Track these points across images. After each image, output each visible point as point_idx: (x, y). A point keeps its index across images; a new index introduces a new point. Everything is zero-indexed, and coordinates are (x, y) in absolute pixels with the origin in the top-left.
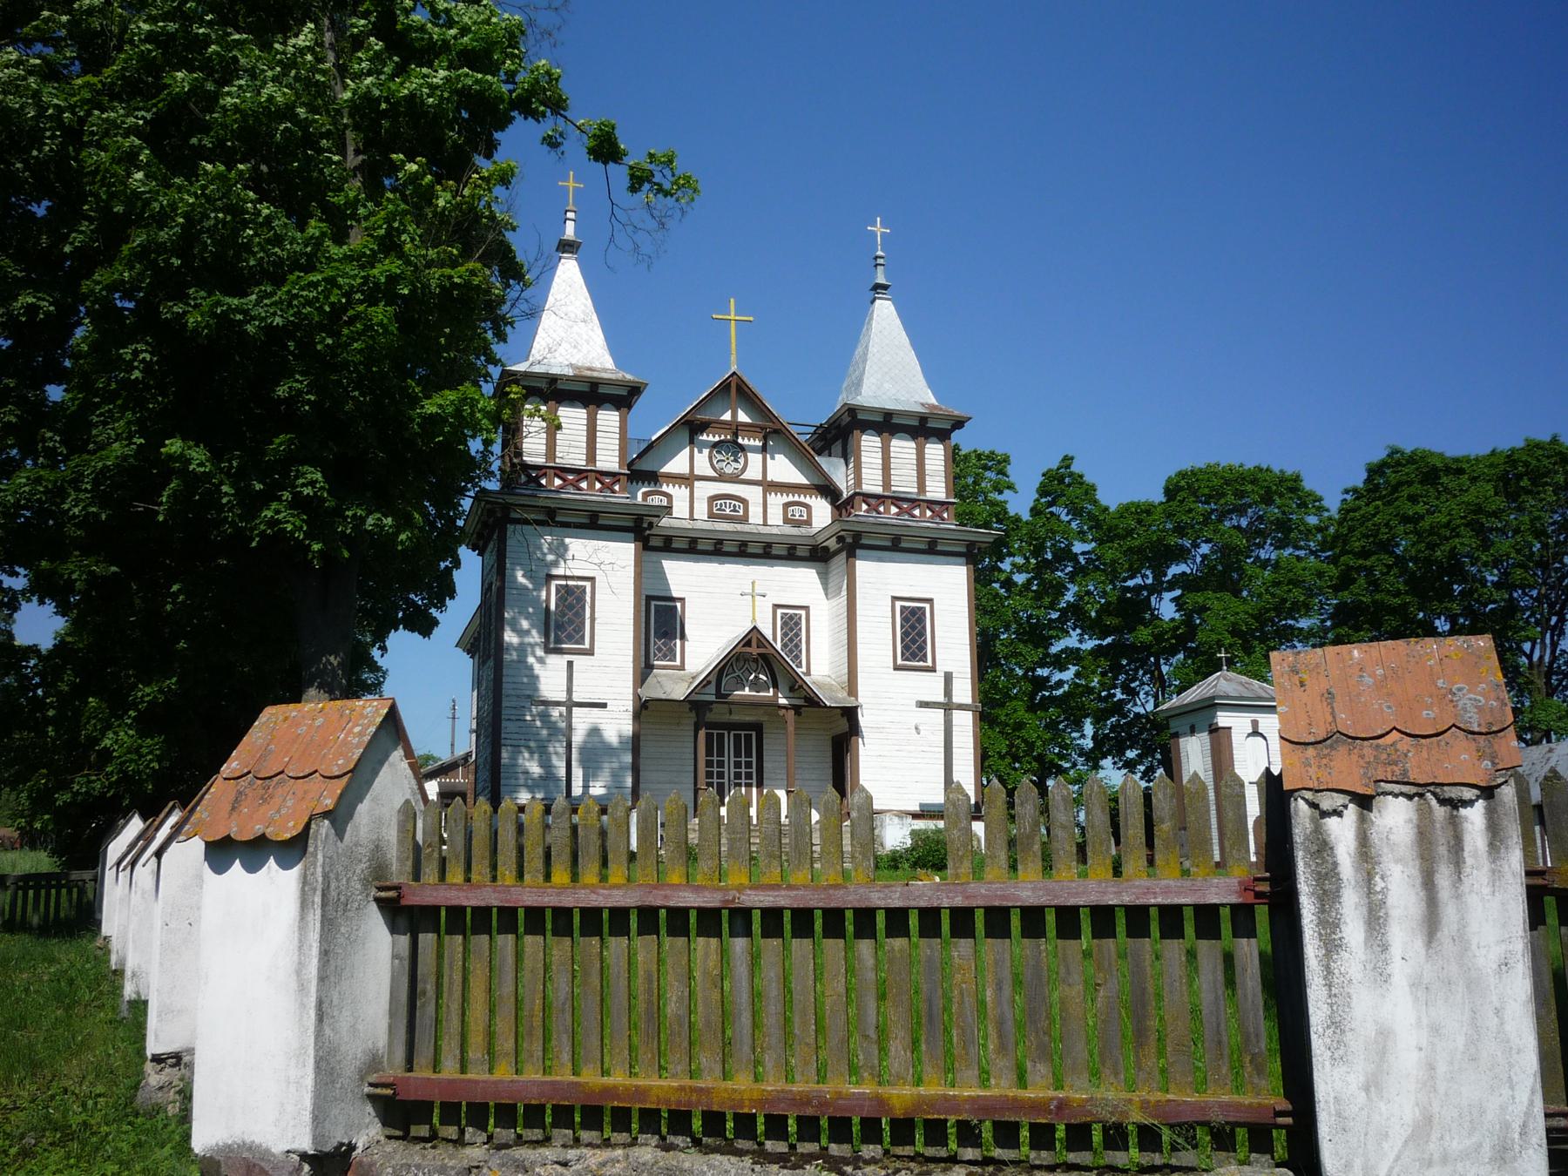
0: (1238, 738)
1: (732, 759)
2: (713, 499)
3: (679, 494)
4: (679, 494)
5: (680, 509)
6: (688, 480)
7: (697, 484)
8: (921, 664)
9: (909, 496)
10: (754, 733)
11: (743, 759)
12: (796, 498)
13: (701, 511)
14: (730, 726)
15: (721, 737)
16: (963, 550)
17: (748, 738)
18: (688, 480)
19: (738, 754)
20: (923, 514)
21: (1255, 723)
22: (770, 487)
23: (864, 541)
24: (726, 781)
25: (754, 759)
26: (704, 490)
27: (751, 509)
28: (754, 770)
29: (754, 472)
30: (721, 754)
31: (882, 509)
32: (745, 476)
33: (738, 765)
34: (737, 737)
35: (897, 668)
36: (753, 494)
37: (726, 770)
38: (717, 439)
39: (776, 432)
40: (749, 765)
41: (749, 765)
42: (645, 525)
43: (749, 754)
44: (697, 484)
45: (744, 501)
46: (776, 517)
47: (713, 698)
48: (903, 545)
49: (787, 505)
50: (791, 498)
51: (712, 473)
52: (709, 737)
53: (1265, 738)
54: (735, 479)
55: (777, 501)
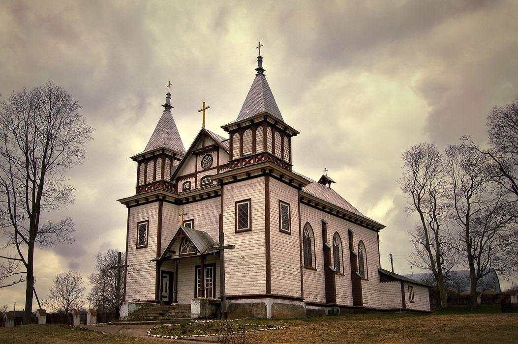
2: (202, 179)
3: (192, 180)
5: (193, 188)
8: (246, 228)
9: (248, 156)
10: (213, 267)
13: (199, 183)
17: (211, 269)
18: (194, 175)
20: (255, 161)
25: (213, 278)
26: (200, 176)
31: (239, 165)
35: (237, 232)
40: (211, 280)
41: (211, 280)
43: (211, 276)
47: (178, 257)
48: (252, 175)
51: (202, 169)
54: (209, 169)
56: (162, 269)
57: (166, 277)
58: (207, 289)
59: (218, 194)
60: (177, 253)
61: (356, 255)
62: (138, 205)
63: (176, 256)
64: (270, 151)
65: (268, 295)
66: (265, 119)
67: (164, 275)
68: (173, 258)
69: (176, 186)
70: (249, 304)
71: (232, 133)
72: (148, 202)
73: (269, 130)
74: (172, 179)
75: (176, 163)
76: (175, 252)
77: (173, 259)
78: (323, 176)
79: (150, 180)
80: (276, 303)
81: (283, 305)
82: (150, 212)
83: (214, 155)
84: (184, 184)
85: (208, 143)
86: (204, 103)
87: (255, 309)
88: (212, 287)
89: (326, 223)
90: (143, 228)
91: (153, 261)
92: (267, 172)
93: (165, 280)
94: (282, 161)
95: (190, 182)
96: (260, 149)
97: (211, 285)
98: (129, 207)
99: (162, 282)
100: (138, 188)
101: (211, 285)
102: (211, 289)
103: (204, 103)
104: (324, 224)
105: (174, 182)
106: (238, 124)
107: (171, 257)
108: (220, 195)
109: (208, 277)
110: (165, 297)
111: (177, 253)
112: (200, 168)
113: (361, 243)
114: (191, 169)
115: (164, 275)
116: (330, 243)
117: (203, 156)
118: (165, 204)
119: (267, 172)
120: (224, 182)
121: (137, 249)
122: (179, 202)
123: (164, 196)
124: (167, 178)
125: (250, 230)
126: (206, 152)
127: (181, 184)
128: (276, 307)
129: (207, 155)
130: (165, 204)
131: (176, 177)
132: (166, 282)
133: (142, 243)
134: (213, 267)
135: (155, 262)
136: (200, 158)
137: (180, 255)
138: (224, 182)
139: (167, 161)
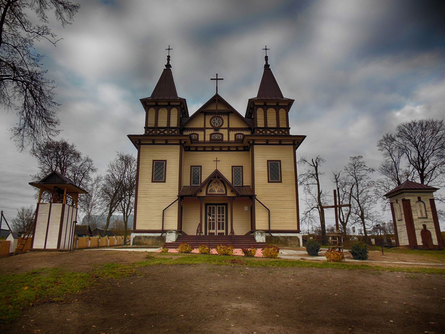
0: (412, 203)
1: (217, 215)
3: (201, 134)
4: (201, 134)
5: (201, 138)
6: (203, 129)
7: (206, 130)
10: (225, 206)
11: (221, 215)
12: (239, 132)
14: (216, 204)
15: (214, 208)
16: (292, 143)
17: (223, 208)
18: (203, 129)
19: (219, 213)
22: (230, 129)
23: (256, 142)
24: (215, 222)
27: (224, 136)
28: (225, 218)
29: (225, 125)
30: (214, 213)
32: (223, 127)
33: (219, 216)
34: (219, 208)
36: (224, 132)
37: (215, 218)
38: (213, 116)
39: (232, 112)
40: (223, 216)
41: (223, 216)
42: (183, 142)
43: (223, 213)
44: (206, 130)
45: (222, 135)
46: (232, 138)
47: (205, 195)
49: (236, 135)
50: (237, 132)
51: (210, 126)
52: (210, 208)
53: (424, 203)
55: (232, 134)
58: (219, 223)
63: (203, 194)
68: (198, 195)
70: (284, 236)
76: (201, 191)
77: (198, 197)
83: (225, 118)
85: (221, 108)
86: (217, 74)
88: (225, 222)
95: (198, 135)
97: (223, 220)
100: (146, 128)
101: (223, 220)
102: (223, 223)
103: (217, 74)
112: (208, 125)
117: (211, 116)
120: (255, 143)
121: (152, 182)
125: (281, 182)
126: (217, 114)
134: (225, 206)
136: (208, 118)
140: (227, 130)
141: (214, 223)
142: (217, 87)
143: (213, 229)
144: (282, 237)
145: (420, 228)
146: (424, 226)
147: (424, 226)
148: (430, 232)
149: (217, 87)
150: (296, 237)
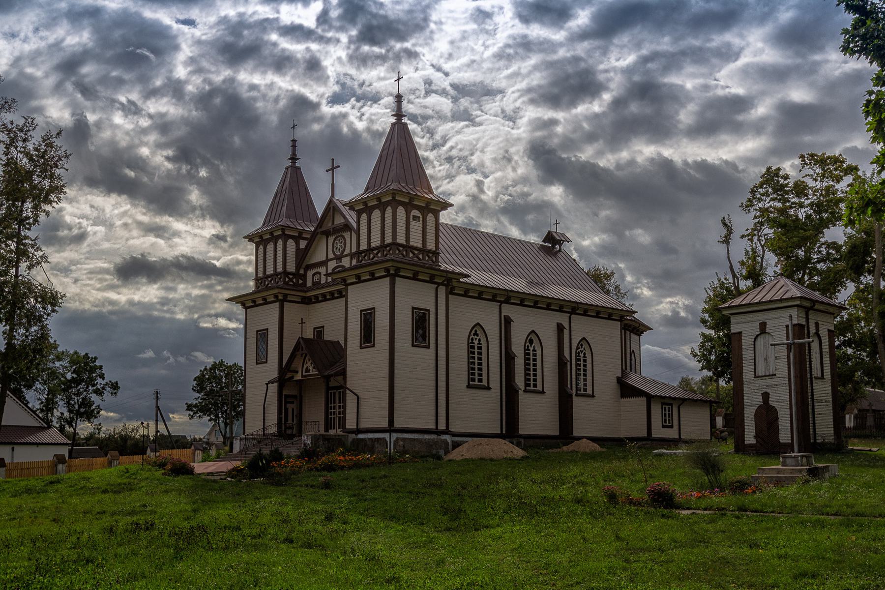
15: (334, 393)
21: (763, 326)
29: (347, 252)
47: (300, 378)
51: (333, 256)
56: (285, 393)
57: (293, 403)
58: (340, 417)
59: (342, 294)
60: (300, 374)
61: (566, 363)
62: (256, 306)
63: (298, 377)
64: (401, 240)
65: (391, 428)
66: (394, 198)
67: (288, 400)
69: (304, 277)
71: (359, 213)
72: (266, 302)
73: (401, 211)
74: (298, 267)
75: (303, 244)
76: (297, 372)
77: (297, 381)
78: (549, 232)
79: (270, 271)
80: (400, 438)
81: (414, 439)
82: (269, 316)
84: (314, 275)
87: (376, 446)
89: (510, 323)
90: (263, 335)
91: (270, 382)
92: (391, 272)
93: (290, 406)
94: (424, 251)
95: (319, 273)
96: (388, 240)
98: (246, 308)
99: (286, 410)
104: (508, 321)
105: (302, 272)
106: (364, 202)
107: (293, 377)
108: (343, 296)
109: (340, 403)
110: (292, 428)
111: (300, 374)
112: (331, 256)
113: (585, 345)
114: (319, 255)
115: (288, 400)
116: (518, 348)
118: (286, 304)
119: (391, 272)
122: (307, 301)
123: (285, 296)
124: (291, 267)
127: (310, 274)
128: (401, 443)
129: (339, 236)
130: (286, 304)
131: (304, 265)
132: (293, 409)
133: (261, 359)
135: (276, 384)
136: (331, 239)
137: (303, 376)
138: (348, 282)
139: (291, 243)
140: (348, 258)
141: (334, 418)
142: (333, 185)
143: (334, 428)
144: (369, 439)
145: (754, 403)
146: (766, 396)
147: (766, 396)
148: (776, 410)
149: (333, 185)
150: (384, 439)
